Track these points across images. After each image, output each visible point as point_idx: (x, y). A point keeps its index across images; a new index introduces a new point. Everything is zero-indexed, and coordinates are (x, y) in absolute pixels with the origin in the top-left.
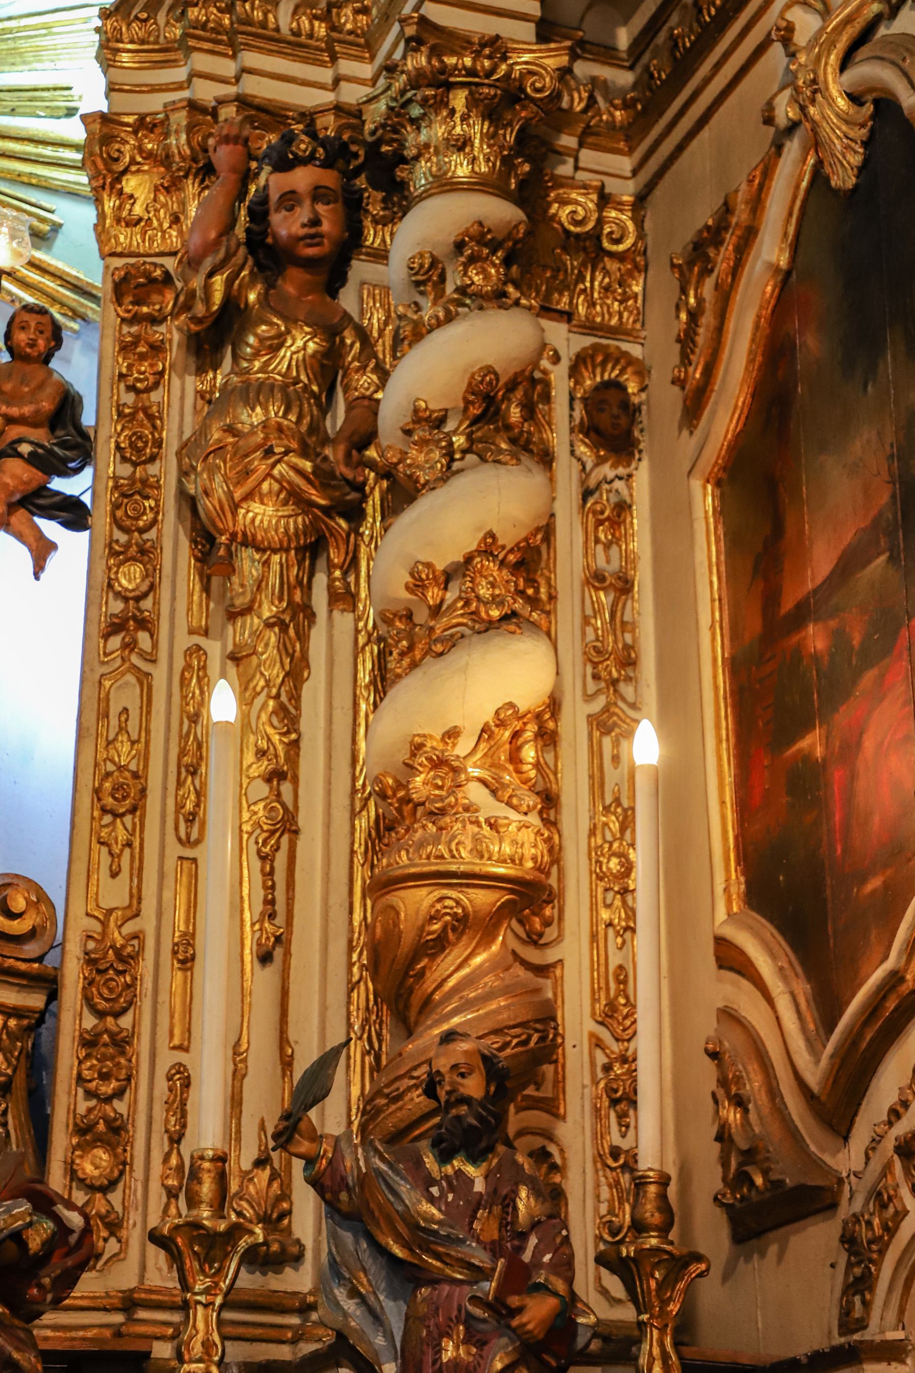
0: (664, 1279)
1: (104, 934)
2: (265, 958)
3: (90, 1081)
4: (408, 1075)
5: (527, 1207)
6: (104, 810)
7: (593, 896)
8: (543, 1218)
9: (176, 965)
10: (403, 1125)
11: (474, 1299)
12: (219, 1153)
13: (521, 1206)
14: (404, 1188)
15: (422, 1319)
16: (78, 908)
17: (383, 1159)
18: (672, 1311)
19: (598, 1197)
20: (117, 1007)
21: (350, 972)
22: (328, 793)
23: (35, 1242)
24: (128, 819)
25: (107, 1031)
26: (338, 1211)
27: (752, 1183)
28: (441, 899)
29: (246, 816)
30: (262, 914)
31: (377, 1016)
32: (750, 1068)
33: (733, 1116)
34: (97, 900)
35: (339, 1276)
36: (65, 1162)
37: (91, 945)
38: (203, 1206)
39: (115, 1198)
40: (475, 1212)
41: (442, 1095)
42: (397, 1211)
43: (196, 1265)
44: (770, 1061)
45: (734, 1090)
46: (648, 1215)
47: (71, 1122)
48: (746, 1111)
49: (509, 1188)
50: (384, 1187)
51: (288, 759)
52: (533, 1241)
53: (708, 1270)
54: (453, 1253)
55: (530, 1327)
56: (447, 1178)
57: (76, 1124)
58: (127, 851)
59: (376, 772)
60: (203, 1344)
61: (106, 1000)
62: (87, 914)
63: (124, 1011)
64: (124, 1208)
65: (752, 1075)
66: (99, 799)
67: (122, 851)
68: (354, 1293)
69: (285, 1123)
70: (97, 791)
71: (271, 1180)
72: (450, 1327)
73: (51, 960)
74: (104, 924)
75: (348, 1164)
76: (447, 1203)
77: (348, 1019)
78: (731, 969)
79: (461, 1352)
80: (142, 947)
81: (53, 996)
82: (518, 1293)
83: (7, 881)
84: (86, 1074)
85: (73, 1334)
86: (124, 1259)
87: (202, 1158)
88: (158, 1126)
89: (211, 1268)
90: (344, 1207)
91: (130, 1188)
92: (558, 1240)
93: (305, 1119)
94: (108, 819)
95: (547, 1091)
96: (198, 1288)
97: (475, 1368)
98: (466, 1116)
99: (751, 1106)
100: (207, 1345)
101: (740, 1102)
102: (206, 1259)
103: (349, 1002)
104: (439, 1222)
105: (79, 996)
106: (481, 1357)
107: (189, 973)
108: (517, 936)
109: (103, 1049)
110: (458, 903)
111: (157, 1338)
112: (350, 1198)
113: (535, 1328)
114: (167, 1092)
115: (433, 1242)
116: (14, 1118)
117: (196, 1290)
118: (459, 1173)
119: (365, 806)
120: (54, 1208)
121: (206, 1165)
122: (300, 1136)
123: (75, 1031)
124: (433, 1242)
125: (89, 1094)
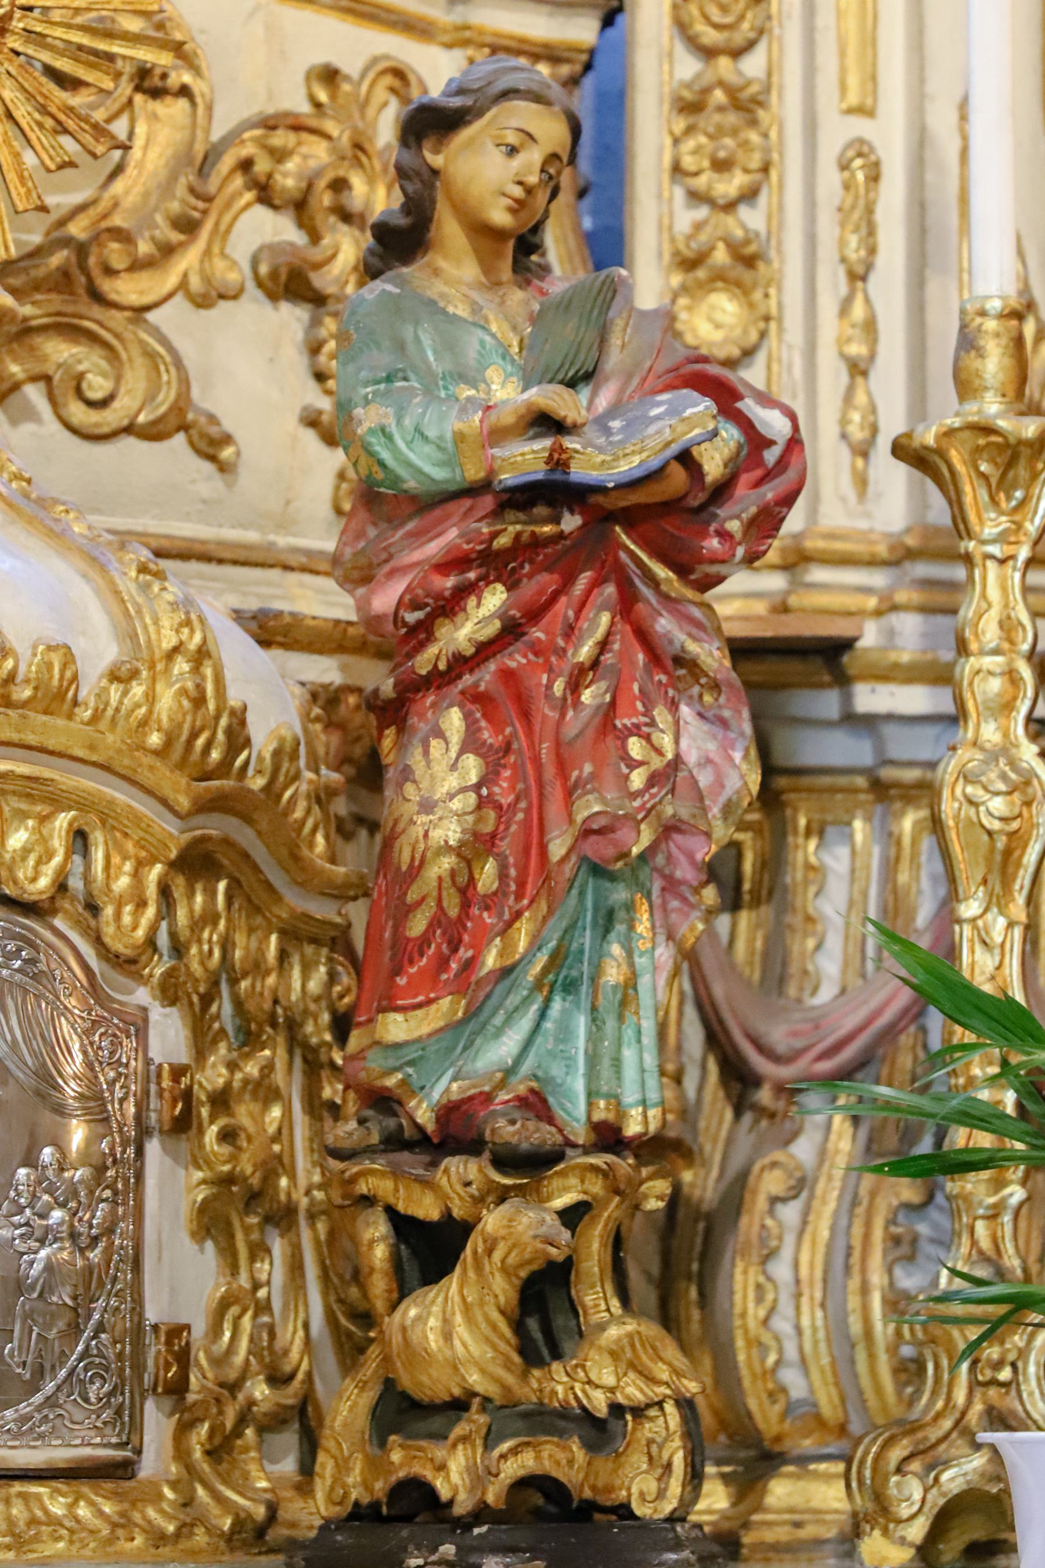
3: (696, 174)
20: (738, 39)
25: (721, 84)
38: (989, 396)
43: (984, 495)
57: (676, 253)
60: (1001, 624)
61: (717, 26)
63: (750, 45)
84: (688, 162)
87: (983, 313)
88: (827, 252)
89: (1009, 498)
91: (780, 361)
100: (1008, 627)
105: (667, 21)
109: (717, 118)
116: (556, 241)
120: (739, 405)
123: (661, 84)
125: (695, 197)
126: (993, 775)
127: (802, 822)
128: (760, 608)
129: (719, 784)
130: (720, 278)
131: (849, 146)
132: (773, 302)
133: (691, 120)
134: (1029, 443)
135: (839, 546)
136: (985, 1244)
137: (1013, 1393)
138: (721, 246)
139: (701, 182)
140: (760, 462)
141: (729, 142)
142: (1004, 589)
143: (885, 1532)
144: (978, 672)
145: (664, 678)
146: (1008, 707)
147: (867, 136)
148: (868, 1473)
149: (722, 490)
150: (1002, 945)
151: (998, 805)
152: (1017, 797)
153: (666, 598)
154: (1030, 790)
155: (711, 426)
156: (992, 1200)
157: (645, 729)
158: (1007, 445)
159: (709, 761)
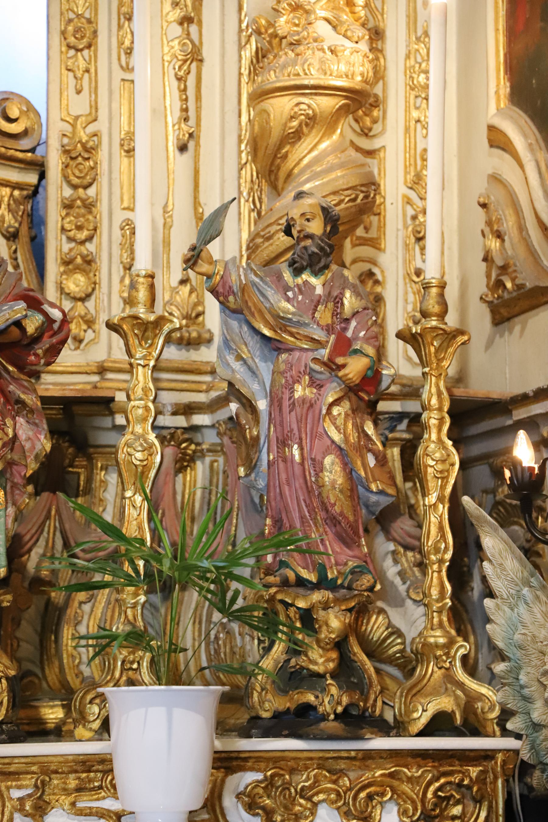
0: (440, 346)
1: (74, 132)
2: (183, 148)
3: (70, 231)
4: (276, 222)
5: (350, 303)
6: (69, 47)
7: (407, 102)
8: (360, 310)
9: (123, 154)
10: (273, 255)
11: (315, 360)
12: (150, 272)
13: (346, 302)
14: (270, 293)
15: (282, 373)
16: (55, 115)
17: (256, 275)
18: (444, 366)
19: (406, 301)
21: (240, 157)
22: (223, 32)
23: (31, 327)
24: (86, 52)
25: (79, 198)
26: (228, 308)
27: (505, 287)
28: (298, 104)
29: (166, 49)
30: (180, 118)
31: (259, 186)
32: (507, 212)
33: (494, 244)
34: (67, 110)
35: (229, 348)
36: (56, 283)
37: (66, 141)
38: (140, 306)
39: (90, 304)
40: (316, 307)
41: (295, 232)
42: (266, 307)
43: (136, 341)
44: (521, 207)
45: (495, 227)
46: (430, 307)
47: (59, 257)
48: (503, 241)
49: (339, 291)
50: (257, 293)
51: (194, 8)
52: (353, 324)
53: (469, 340)
54: (301, 332)
55: (350, 376)
56: (298, 285)
57: (62, 259)
58: (86, 75)
59: (253, 15)
60: (143, 389)
61: (78, 177)
62: (62, 120)
63: (90, 185)
64: (96, 311)
65: (508, 218)
66: (65, 39)
67: (83, 75)
68: (239, 358)
69: (192, 253)
70: (63, 33)
71: (191, 292)
72: (299, 377)
73: (40, 151)
74: (74, 126)
75: (233, 278)
76: (298, 302)
77: (239, 188)
78: (498, 147)
79: (307, 391)
80: (100, 142)
81: (42, 176)
82: (343, 355)
83: (5, 96)
84: (67, 226)
85: (67, 387)
86: (98, 343)
87: (138, 276)
89: (146, 343)
90: (232, 305)
91: (99, 298)
92: (370, 323)
93: (205, 250)
94: (72, 52)
95: (373, 234)
96: (138, 356)
97: (315, 401)
98: (310, 246)
99: (506, 238)
100: (145, 390)
101: (499, 236)
102: (142, 338)
103: (239, 177)
104: (293, 314)
105: (60, 175)
106: (320, 395)
107: (132, 159)
108: (354, 131)
109: (77, 210)
110: (309, 106)
111: (120, 390)
112: (236, 300)
113: (353, 377)
114: (121, 238)
115: (289, 326)
116: (21, 255)
117: (137, 357)
118: (306, 283)
119: (248, 41)
120: (42, 307)
121: (141, 280)
122: (202, 261)
123: (58, 198)
124: (289, 326)
125: (70, 239)
126: (137, 444)
127: (99, 465)
128: (89, 387)
129: (33, 447)
130: (78, 269)
131: (124, 221)
132: (97, 278)
133: (68, 211)
134: (152, 323)
135: (117, 365)
136: (131, 617)
137: (138, 673)
138: (79, 257)
139: (71, 234)
140: (52, 328)
141: (82, 219)
142: (145, 377)
143: (84, 726)
144: (134, 407)
145: (10, 408)
146: (145, 420)
147: (131, 218)
148: (77, 704)
149: (36, 339)
150: (141, 507)
151: (139, 455)
152: (146, 452)
153: (13, 378)
154: (152, 450)
155: (24, 313)
156: (133, 601)
157: (2, 426)
158: (144, 323)
159: (29, 439)
